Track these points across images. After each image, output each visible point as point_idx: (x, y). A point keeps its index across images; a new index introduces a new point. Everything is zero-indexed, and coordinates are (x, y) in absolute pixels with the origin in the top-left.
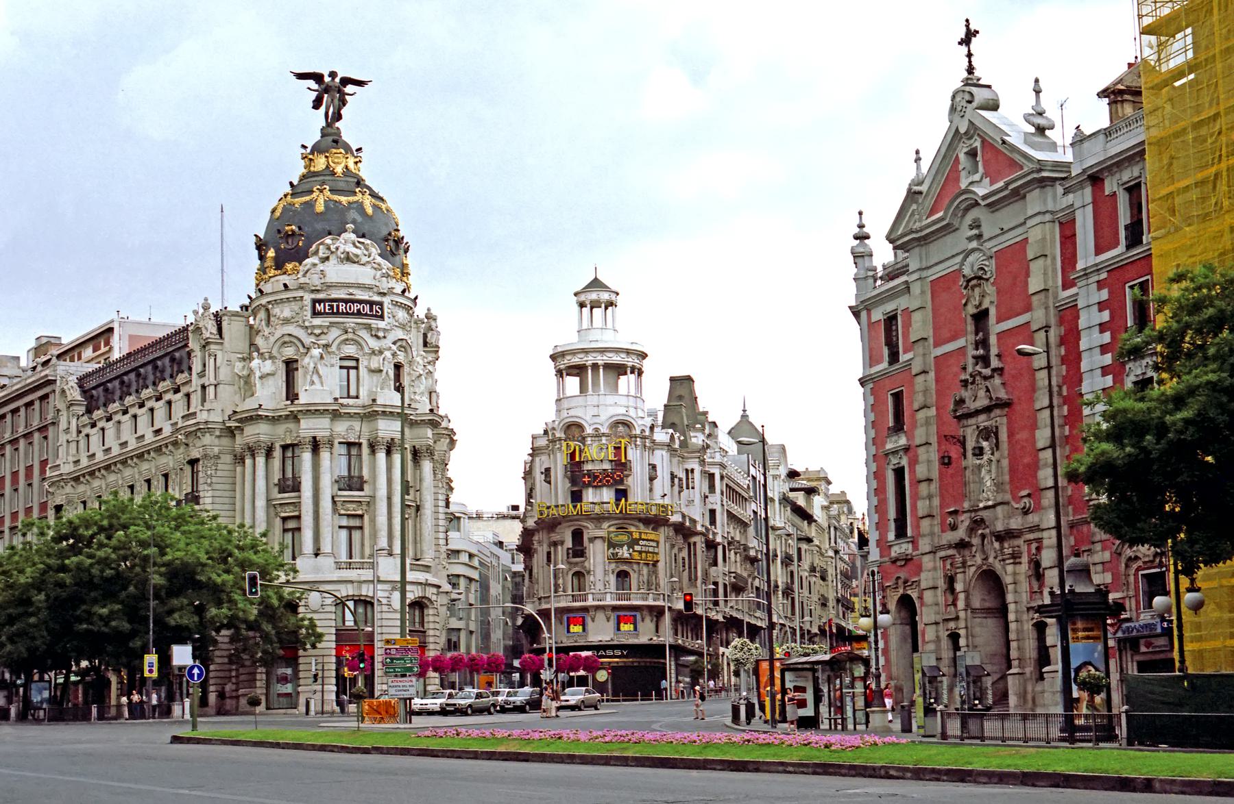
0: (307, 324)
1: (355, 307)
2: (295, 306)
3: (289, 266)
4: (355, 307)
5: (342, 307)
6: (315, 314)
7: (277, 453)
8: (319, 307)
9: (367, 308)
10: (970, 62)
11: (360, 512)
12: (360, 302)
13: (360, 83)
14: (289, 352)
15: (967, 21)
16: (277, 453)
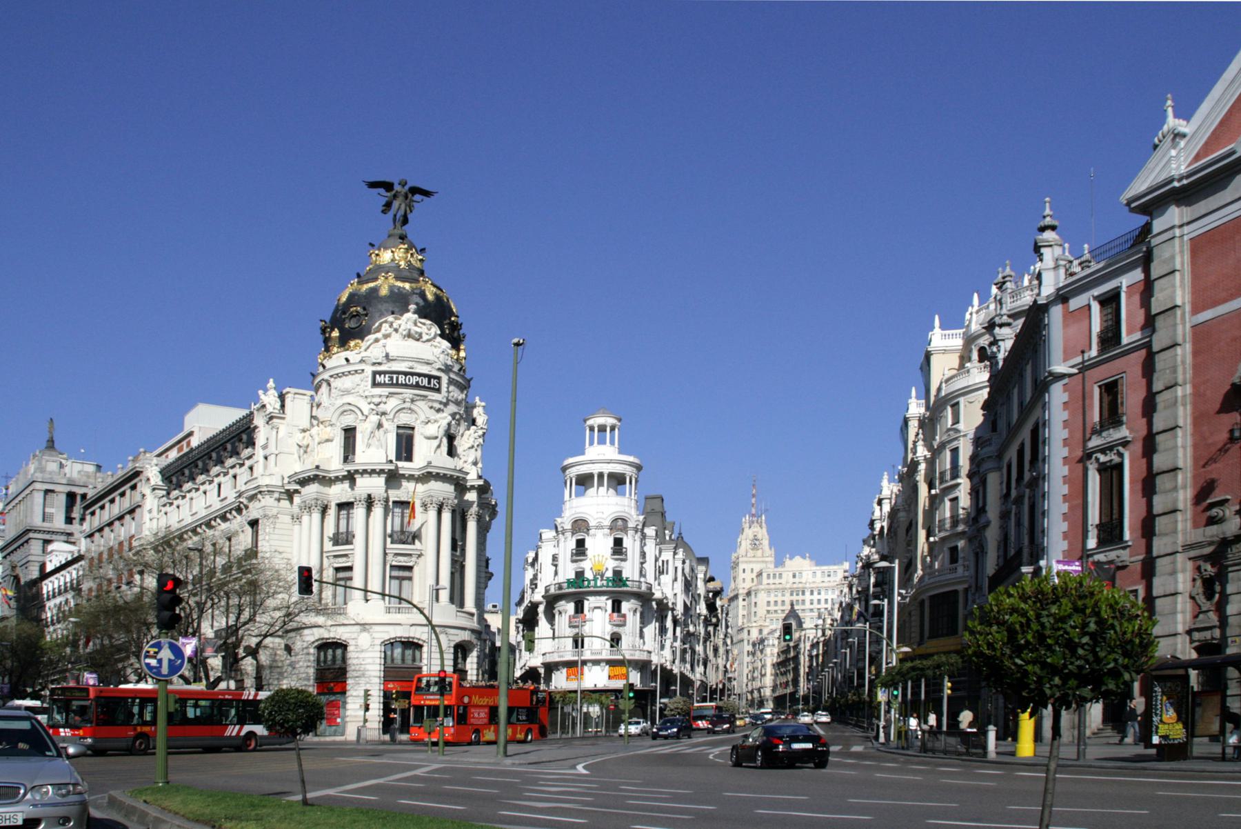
0: (367, 393)
1: (414, 380)
2: (357, 377)
3: (352, 343)
4: (414, 380)
5: (402, 379)
6: (375, 384)
7: (332, 512)
8: (379, 379)
9: (425, 382)
11: (411, 564)
12: (419, 375)
13: (426, 193)
14: (348, 421)
16: (332, 512)
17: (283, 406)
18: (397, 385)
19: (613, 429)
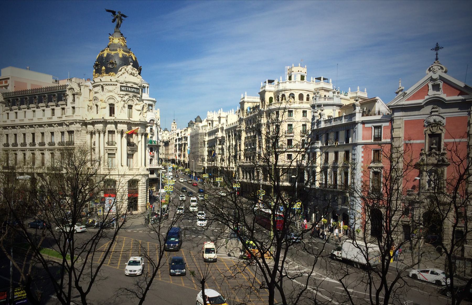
0: (118, 93)
1: (133, 90)
2: (114, 87)
3: (112, 74)
4: (133, 90)
6: (121, 90)
7: (107, 133)
8: (123, 88)
9: (136, 90)
10: (437, 56)
12: (134, 88)
15: (437, 43)
16: (107, 133)
17: (80, 90)
18: (128, 91)
19: (148, 87)
